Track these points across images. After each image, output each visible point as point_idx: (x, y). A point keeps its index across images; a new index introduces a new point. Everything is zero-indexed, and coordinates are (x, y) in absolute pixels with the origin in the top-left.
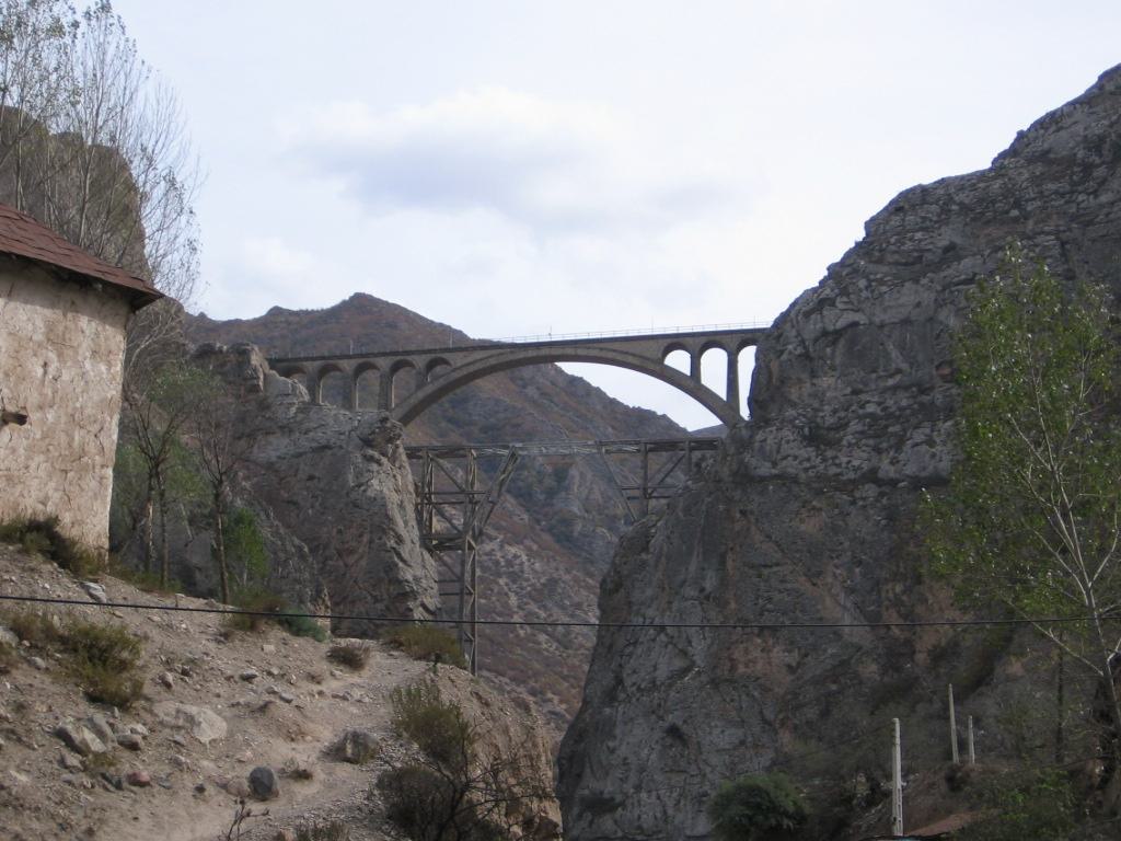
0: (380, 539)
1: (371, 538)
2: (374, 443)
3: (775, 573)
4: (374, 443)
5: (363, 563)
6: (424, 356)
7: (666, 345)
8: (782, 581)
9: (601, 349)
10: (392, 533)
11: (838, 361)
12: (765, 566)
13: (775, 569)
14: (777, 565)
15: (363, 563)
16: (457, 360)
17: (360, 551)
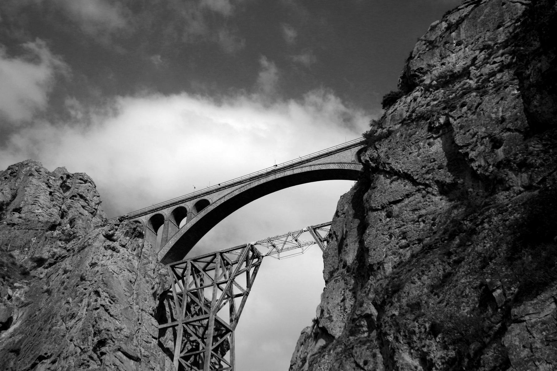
0: (96, 301)
1: (88, 302)
2: (115, 238)
3: (406, 206)
4: (115, 238)
5: (80, 324)
6: (192, 201)
7: (357, 150)
8: (416, 210)
9: (310, 166)
10: (105, 294)
11: (463, 36)
12: (396, 202)
13: (406, 201)
14: (408, 196)
15: (80, 324)
16: (212, 198)
17: (79, 314)
